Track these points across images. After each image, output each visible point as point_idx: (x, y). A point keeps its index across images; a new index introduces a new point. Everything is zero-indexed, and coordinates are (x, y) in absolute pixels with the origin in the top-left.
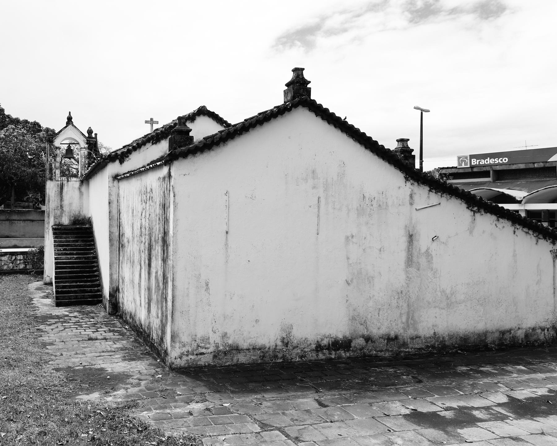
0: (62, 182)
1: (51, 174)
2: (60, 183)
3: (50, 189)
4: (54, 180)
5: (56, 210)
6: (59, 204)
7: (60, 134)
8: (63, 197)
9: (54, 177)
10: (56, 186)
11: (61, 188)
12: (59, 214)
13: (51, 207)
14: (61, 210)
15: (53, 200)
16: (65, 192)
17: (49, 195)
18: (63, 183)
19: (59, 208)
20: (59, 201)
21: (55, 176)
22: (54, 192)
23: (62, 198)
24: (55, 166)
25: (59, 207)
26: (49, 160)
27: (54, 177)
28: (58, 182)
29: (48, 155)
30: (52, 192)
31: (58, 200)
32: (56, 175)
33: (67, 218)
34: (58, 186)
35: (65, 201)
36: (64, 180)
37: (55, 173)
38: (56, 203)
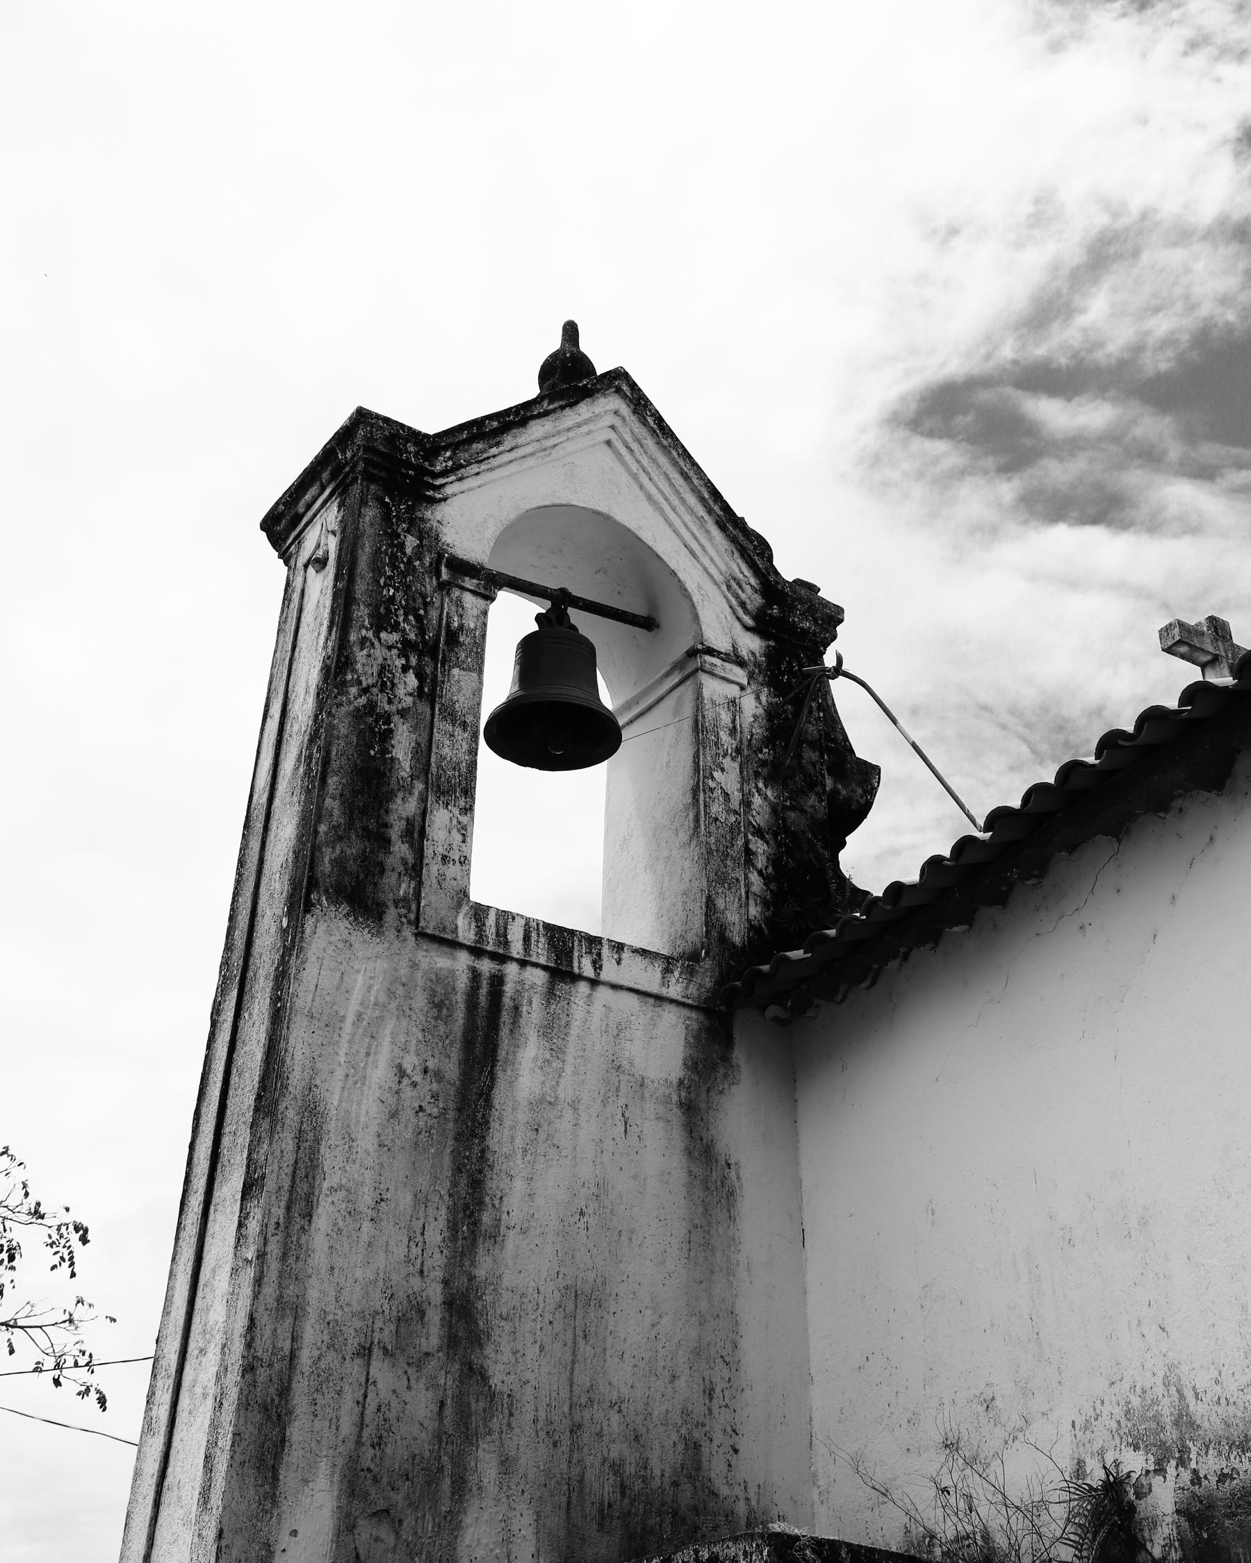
0: (486, 966)
1: (367, 834)
2: (462, 982)
3: (332, 1024)
4: (391, 915)
5: (379, 1368)
6: (437, 1261)
7: (508, 441)
8: (493, 1185)
9: (405, 888)
10: (420, 1000)
11: (468, 1043)
12: (424, 1443)
13: (317, 1294)
14: (448, 1381)
15: (366, 1199)
16: (523, 1116)
17: (312, 1110)
18: (497, 981)
19: (432, 1335)
20: (435, 1235)
21: (416, 870)
22: (380, 1073)
23: (477, 1184)
24: (423, 753)
25: (435, 1316)
26: (365, 664)
27: (405, 888)
28: (441, 961)
29: (362, 613)
30: (356, 1077)
31: (421, 1200)
32: (433, 869)
33: (524, 1523)
34: (439, 1005)
35: (512, 1241)
36: (517, 949)
37: (417, 833)
38: (401, 1252)
